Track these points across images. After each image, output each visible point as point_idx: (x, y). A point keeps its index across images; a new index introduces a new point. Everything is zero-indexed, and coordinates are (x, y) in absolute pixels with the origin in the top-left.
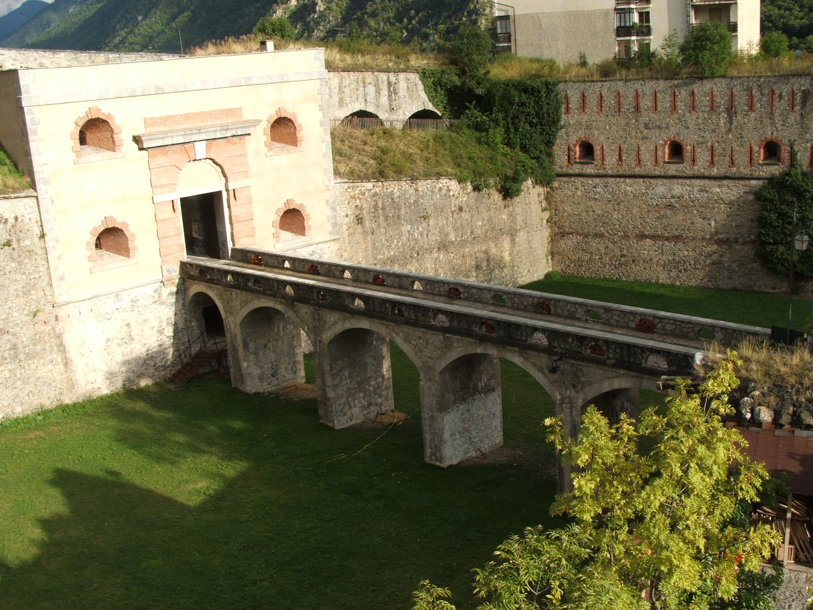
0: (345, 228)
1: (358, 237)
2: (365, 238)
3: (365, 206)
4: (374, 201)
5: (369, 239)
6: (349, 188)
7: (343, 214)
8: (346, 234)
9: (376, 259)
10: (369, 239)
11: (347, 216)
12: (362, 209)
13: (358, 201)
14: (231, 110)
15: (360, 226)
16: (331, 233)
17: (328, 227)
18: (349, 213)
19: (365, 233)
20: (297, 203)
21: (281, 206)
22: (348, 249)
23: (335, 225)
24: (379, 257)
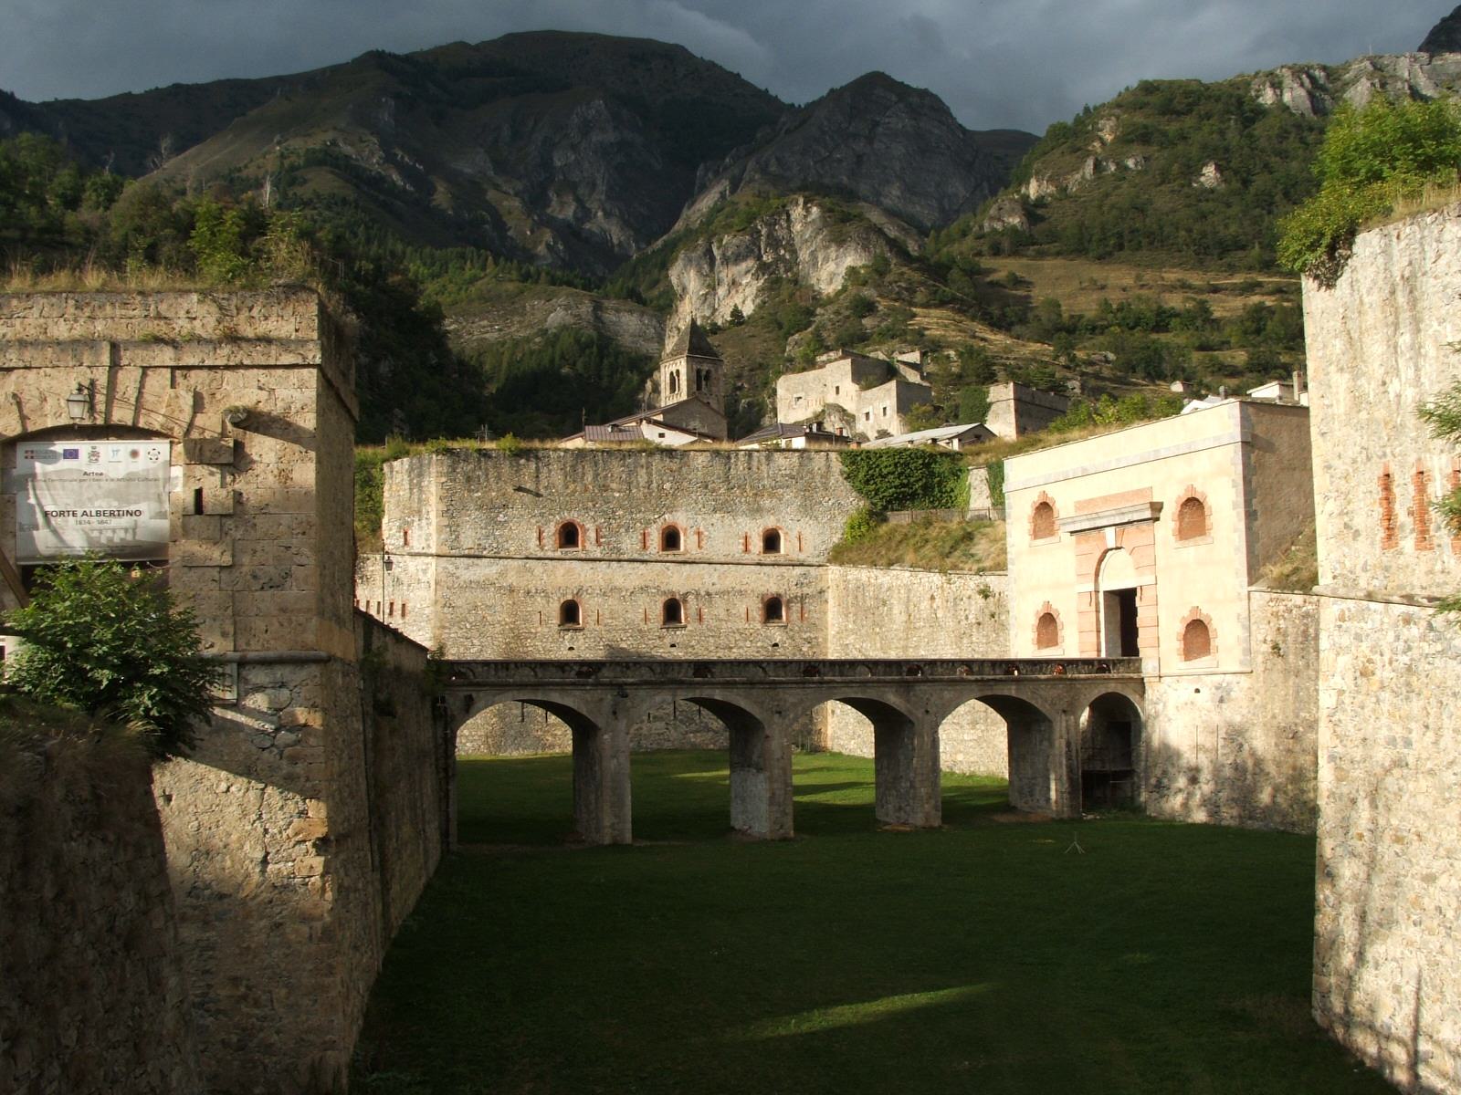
0: (1260, 659)
1: (1277, 677)
2: (1286, 681)
3: (1290, 630)
4: (1306, 625)
5: (1291, 683)
6: (1271, 600)
7: (1261, 638)
8: (1261, 668)
9: (1297, 717)
10: (1291, 683)
11: (1265, 641)
12: (1285, 635)
13: (1282, 622)
14: (1141, 490)
15: (1280, 659)
16: (1241, 663)
17: (1238, 653)
18: (1269, 638)
19: (1286, 672)
20: (1207, 611)
21: (1186, 614)
22: (1262, 691)
23: (1248, 651)
24: (1302, 714)
